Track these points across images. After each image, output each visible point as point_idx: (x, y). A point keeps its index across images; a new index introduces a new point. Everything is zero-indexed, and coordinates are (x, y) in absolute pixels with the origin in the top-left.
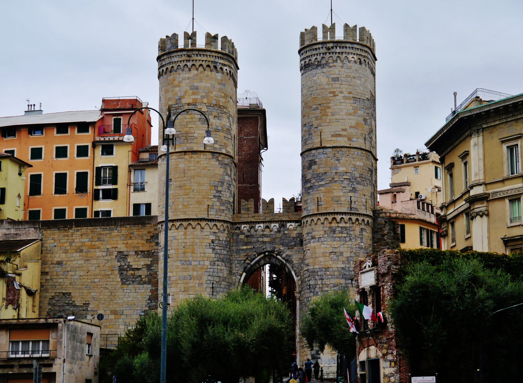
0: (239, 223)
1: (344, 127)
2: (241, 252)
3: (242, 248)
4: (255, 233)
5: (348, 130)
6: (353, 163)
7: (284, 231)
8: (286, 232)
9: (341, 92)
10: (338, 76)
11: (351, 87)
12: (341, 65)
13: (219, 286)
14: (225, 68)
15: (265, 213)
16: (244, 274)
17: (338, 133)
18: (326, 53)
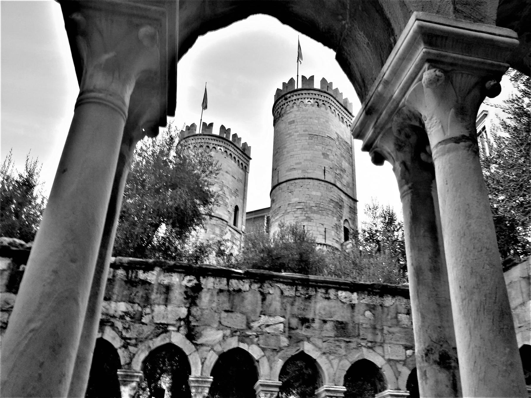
1: (298, 161)
5: (303, 163)
6: (308, 192)
9: (297, 132)
10: (294, 119)
11: (307, 126)
12: (297, 109)
14: (219, 148)
17: (292, 167)
18: (284, 104)
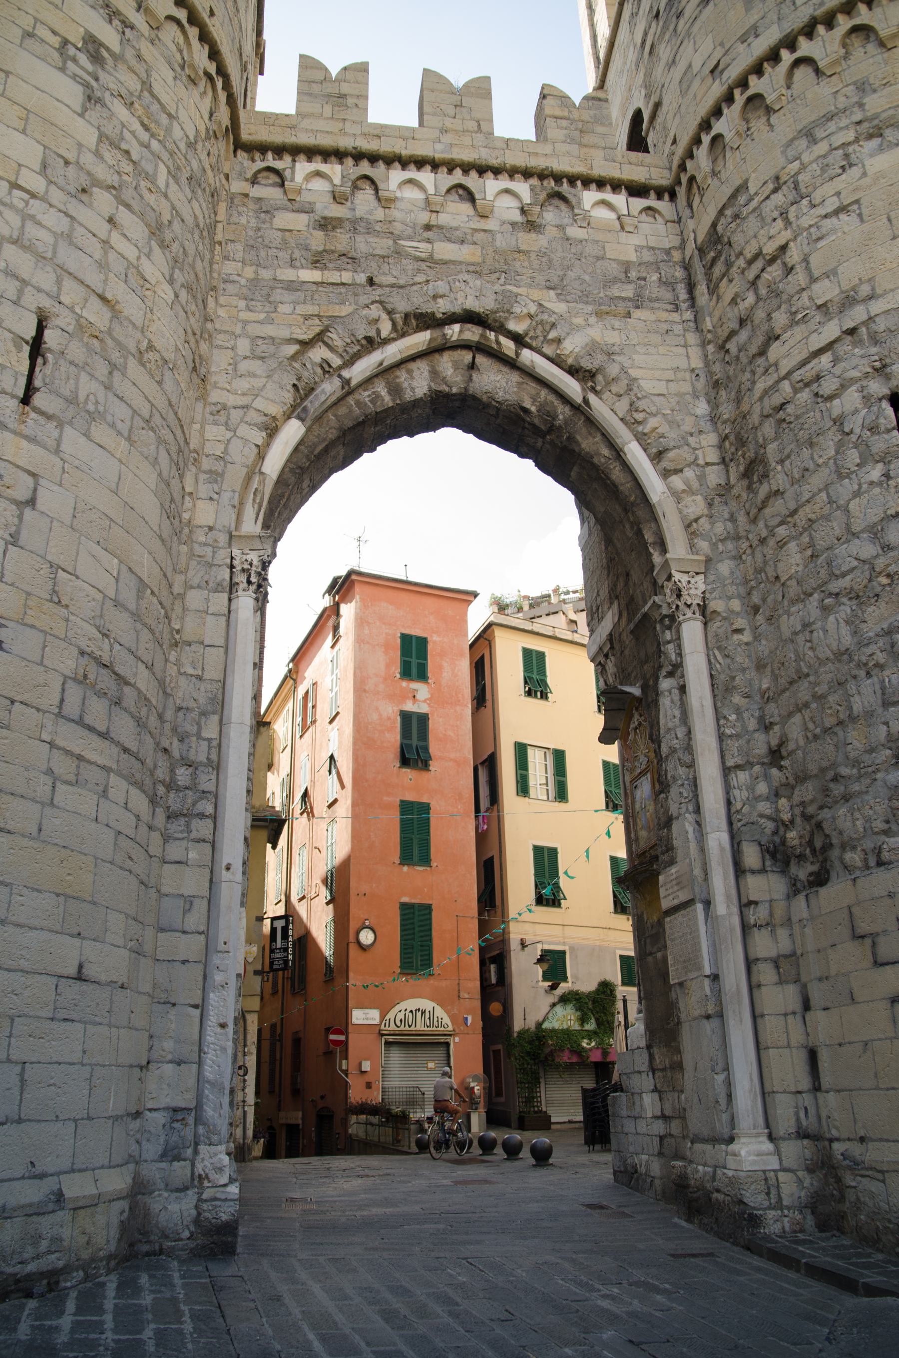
0: (279, 150)
2: (278, 295)
3: (288, 274)
4: (380, 214)
7: (561, 227)
8: (574, 232)
13: (102, 369)
15: (444, 131)
16: (292, 432)
